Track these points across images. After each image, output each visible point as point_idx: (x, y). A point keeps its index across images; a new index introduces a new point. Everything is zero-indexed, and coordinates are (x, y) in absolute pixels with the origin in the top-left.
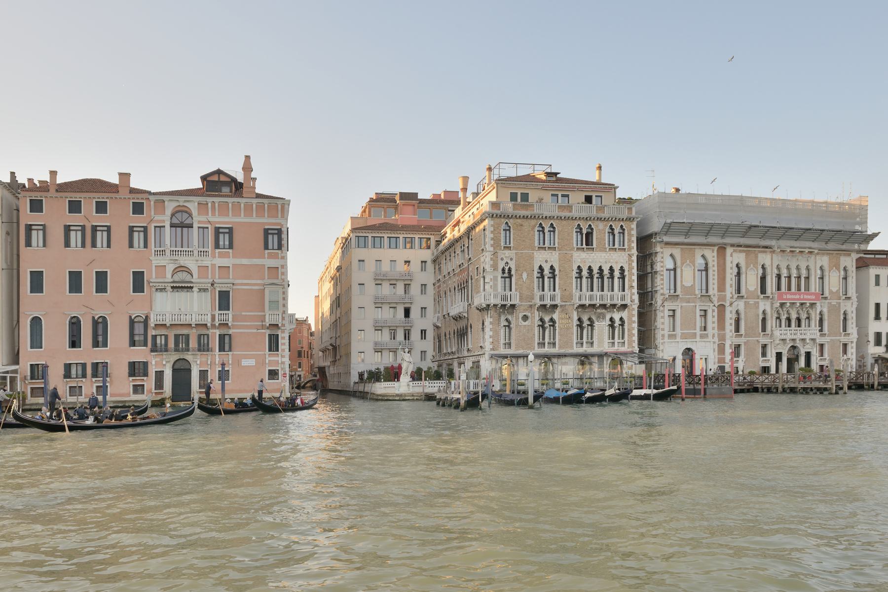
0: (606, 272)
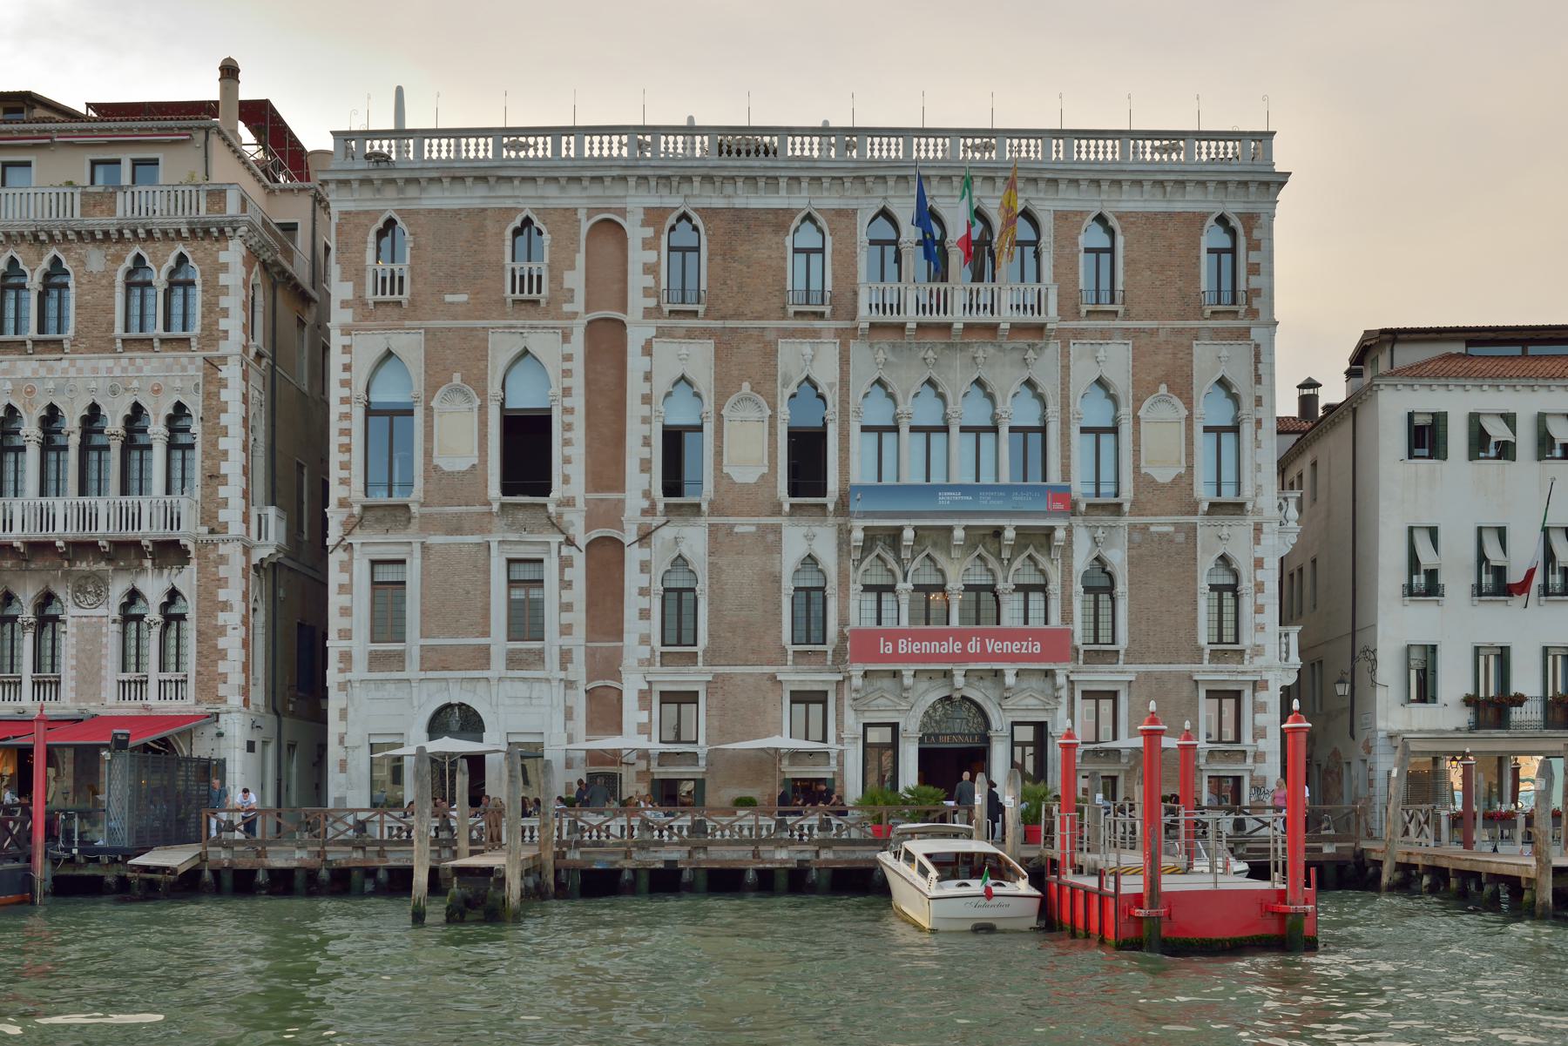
0: (114, 423)
